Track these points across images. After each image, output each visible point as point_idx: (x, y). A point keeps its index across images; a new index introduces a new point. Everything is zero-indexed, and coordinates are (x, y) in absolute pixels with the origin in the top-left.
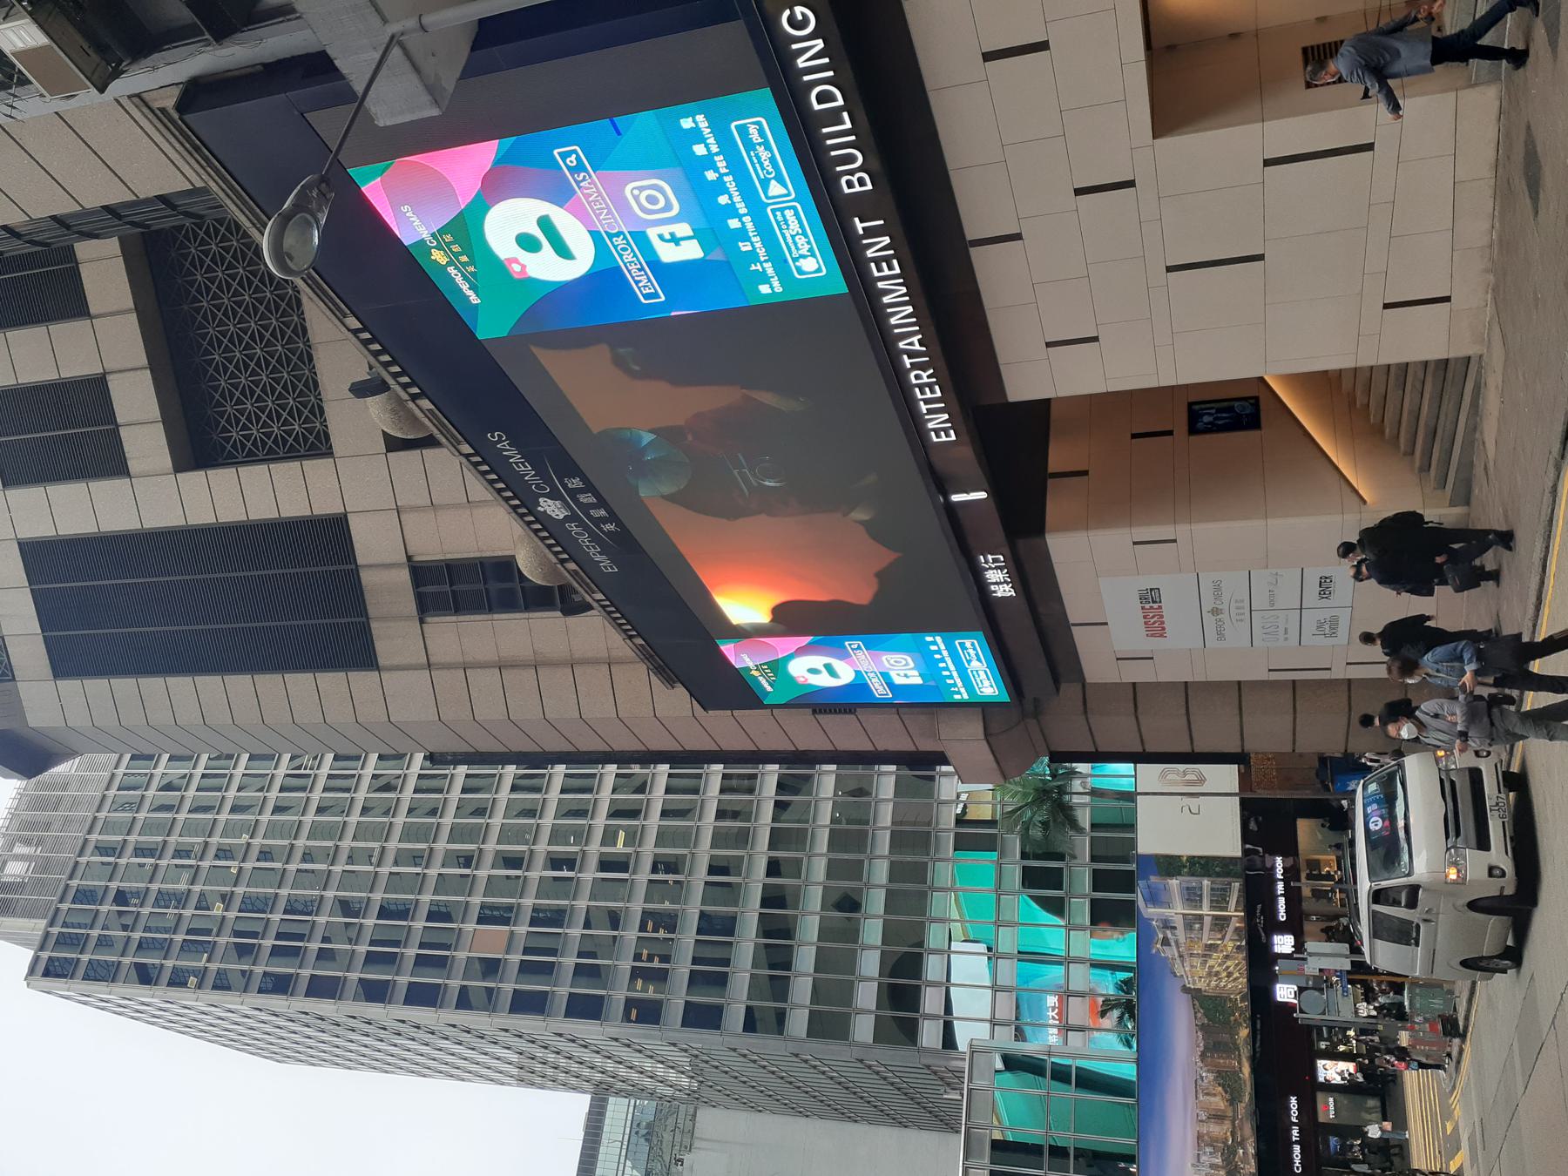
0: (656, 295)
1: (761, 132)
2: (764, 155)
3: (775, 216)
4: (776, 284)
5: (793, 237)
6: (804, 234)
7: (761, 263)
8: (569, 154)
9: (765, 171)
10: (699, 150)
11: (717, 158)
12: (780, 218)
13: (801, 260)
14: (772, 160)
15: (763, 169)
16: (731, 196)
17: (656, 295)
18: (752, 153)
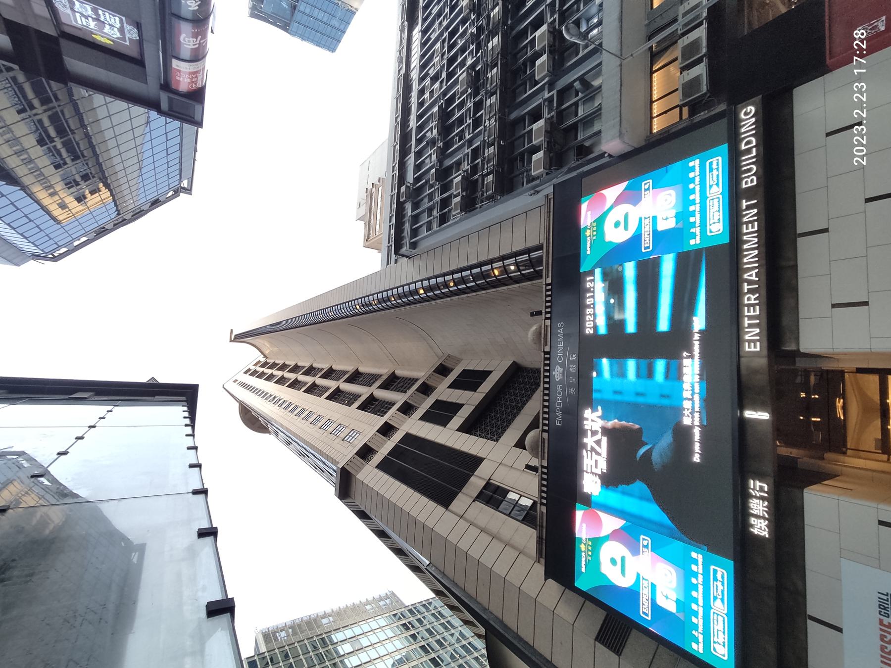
0: (647, 615)
1: (723, 577)
2: (720, 588)
3: (714, 615)
4: (701, 646)
5: (718, 630)
6: (724, 633)
7: (698, 633)
8: (646, 540)
9: (717, 594)
10: (694, 568)
11: (699, 575)
12: (715, 618)
13: (717, 644)
14: (723, 591)
15: (717, 592)
16: (699, 595)
17: (647, 615)
18: (715, 582)
